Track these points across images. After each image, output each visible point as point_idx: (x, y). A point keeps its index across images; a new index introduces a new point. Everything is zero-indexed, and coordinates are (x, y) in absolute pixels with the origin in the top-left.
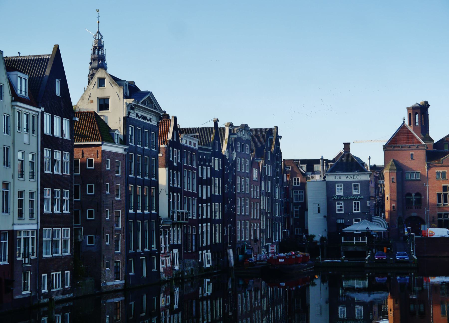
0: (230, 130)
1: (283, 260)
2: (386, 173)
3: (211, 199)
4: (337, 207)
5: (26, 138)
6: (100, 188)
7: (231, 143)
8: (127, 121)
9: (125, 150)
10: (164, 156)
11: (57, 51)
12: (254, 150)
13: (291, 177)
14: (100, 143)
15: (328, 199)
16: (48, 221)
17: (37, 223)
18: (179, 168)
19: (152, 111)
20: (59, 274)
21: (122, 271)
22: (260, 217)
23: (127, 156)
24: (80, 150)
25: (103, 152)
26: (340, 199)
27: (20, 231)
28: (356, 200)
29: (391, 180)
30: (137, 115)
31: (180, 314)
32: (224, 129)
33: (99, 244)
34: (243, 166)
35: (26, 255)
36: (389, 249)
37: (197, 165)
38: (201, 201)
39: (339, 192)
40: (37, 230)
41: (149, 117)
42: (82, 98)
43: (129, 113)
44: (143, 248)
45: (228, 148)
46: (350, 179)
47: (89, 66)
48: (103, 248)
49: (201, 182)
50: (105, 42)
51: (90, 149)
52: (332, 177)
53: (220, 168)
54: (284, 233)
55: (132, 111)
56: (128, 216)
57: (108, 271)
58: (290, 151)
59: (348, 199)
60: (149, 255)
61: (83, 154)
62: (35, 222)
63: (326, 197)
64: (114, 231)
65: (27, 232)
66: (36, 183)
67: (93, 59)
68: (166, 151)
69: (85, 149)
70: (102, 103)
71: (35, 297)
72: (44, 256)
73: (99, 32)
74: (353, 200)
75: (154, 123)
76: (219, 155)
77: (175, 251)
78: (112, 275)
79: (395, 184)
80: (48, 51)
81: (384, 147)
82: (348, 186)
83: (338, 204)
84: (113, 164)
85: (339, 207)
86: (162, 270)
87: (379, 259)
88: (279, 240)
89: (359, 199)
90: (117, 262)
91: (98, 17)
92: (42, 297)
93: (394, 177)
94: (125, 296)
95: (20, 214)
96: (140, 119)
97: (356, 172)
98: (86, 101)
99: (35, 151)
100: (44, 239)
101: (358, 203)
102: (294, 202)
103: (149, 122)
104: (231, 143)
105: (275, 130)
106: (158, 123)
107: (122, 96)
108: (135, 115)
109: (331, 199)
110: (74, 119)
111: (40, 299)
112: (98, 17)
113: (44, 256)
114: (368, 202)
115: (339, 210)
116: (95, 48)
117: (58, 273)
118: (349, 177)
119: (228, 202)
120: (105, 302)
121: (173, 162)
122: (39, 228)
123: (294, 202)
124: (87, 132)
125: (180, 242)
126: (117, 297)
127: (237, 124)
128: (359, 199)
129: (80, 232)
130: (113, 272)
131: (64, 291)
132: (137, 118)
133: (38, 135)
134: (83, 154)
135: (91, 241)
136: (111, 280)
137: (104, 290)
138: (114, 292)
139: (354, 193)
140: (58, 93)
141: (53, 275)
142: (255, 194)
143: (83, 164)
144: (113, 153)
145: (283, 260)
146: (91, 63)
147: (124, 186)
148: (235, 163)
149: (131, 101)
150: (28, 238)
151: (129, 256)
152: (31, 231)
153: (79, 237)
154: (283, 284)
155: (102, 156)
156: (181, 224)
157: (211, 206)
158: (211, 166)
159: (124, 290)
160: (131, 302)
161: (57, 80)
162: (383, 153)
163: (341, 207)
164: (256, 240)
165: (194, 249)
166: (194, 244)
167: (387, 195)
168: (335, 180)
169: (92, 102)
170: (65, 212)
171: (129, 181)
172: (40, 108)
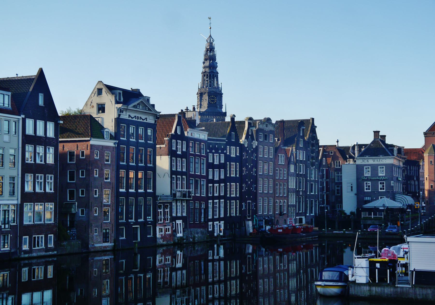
0: (249, 124)
1: (281, 231)
2: (426, 155)
3: (227, 180)
4: (380, 186)
5: (6, 138)
6: (89, 173)
7: (250, 134)
8: (118, 121)
9: (115, 144)
10: (167, 146)
11: (41, 73)
12: (280, 139)
13: (332, 160)
14: (89, 139)
15: (358, 179)
16: (27, 198)
17: (18, 199)
18: (185, 155)
19: (146, 112)
20: (42, 237)
21: (112, 236)
22: (288, 195)
23: (118, 148)
24: (62, 144)
25: (92, 146)
26: (368, 180)
28: (381, 180)
29: (430, 163)
30: (129, 116)
31: (184, 272)
32: (244, 122)
33: (88, 215)
34: (266, 152)
36: (402, 223)
37: (207, 153)
38: (209, 181)
39: (367, 174)
40: (17, 204)
41: (144, 117)
42: (86, 104)
43: (119, 115)
44: (136, 219)
45: (247, 138)
46: (376, 162)
47: (202, 65)
48: (91, 218)
49: (211, 166)
50: (216, 45)
51: (82, 143)
52: (361, 161)
53: (238, 154)
54: (322, 209)
55: (121, 113)
56: (118, 194)
57: (96, 236)
58: (325, 138)
59: (375, 180)
60: (144, 225)
61: (77, 147)
62: (16, 198)
63: (356, 178)
64: (103, 206)
66: (17, 170)
67: (206, 60)
68: (169, 143)
69: (78, 143)
70: (100, 106)
71: (15, 253)
73: (210, 36)
74: (379, 180)
75: (153, 122)
76: (237, 143)
77: (179, 222)
78: (101, 239)
79: (433, 166)
80: (34, 73)
81: (425, 134)
82: (374, 168)
83: (366, 183)
84: (102, 155)
85: (367, 187)
86: (158, 235)
87: (371, 231)
88: (315, 213)
89: (384, 180)
90: (106, 229)
91: (210, 24)
92: (23, 253)
93: (433, 160)
94: (114, 255)
96: (134, 119)
97: (381, 157)
98: (89, 106)
99: (16, 147)
101: (383, 183)
102: (336, 181)
103: (145, 121)
104: (250, 134)
105: (311, 121)
106: (155, 121)
107: (114, 102)
108: (128, 116)
109: (360, 180)
110: (58, 122)
112: (210, 24)
114: (392, 182)
115: (381, 189)
116: (207, 50)
117: (40, 236)
118: (376, 160)
119: (247, 182)
120: (93, 259)
121: (177, 150)
122: (19, 202)
123: (336, 181)
124: (81, 130)
125: (185, 214)
126: (105, 255)
127: (258, 116)
128: (384, 180)
129: (74, 206)
130: (102, 237)
131: (47, 249)
132: (130, 119)
133: (19, 135)
134: (77, 147)
135: (82, 213)
136: (100, 243)
137: (92, 250)
138: (104, 251)
139: (380, 175)
140: (41, 102)
141: (35, 238)
142: (281, 175)
143: (78, 156)
144: (102, 146)
145: (281, 231)
146: (204, 63)
147: (114, 171)
148: (256, 150)
149: (120, 106)
151: (118, 225)
153: (73, 209)
154: (281, 250)
155: (91, 149)
156: (187, 200)
157: (226, 187)
158: (225, 154)
159: (114, 251)
160: (122, 259)
162: (424, 138)
163: (383, 186)
164: (281, 214)
165: (202, 220)
166: (203, 216)
167: (426, 175)
168: (364, 163)
169: (93, 107)
171: (119, 167)
172: (20, 116)
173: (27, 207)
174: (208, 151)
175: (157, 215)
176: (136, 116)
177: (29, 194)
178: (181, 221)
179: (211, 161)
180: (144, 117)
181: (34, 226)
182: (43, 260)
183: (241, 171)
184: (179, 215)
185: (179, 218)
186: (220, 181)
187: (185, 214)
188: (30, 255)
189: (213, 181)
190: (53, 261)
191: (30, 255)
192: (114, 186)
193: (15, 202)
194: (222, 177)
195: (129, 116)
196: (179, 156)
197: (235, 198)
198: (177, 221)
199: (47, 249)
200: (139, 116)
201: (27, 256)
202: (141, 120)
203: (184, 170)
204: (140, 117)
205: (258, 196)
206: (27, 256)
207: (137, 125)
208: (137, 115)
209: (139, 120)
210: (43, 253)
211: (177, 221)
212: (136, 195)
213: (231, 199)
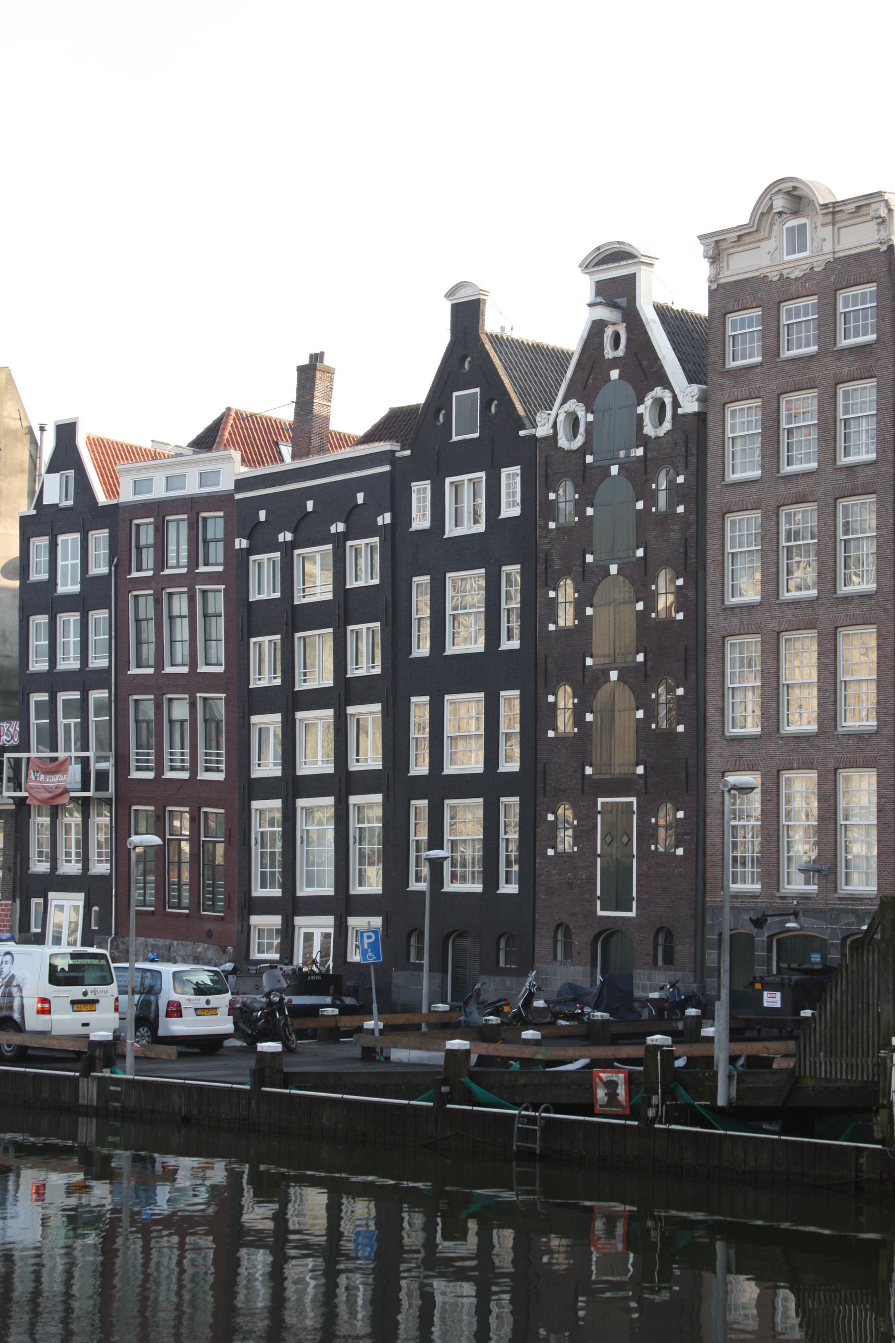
18: (92, 595)
174: (241, 543)
178: (82, 896)
179: (263, 588)
183: (535, 610)
184: (71, 867)
185: (67, 884)
186: (344, 693)
187: (101, 868)
189: (289, 701)
194: (366, 664)
197: (487, 785)
198: (51, 895)
203: (99, 661)
205: (714, 760)
211: (51, 895)
213: (442, 787)
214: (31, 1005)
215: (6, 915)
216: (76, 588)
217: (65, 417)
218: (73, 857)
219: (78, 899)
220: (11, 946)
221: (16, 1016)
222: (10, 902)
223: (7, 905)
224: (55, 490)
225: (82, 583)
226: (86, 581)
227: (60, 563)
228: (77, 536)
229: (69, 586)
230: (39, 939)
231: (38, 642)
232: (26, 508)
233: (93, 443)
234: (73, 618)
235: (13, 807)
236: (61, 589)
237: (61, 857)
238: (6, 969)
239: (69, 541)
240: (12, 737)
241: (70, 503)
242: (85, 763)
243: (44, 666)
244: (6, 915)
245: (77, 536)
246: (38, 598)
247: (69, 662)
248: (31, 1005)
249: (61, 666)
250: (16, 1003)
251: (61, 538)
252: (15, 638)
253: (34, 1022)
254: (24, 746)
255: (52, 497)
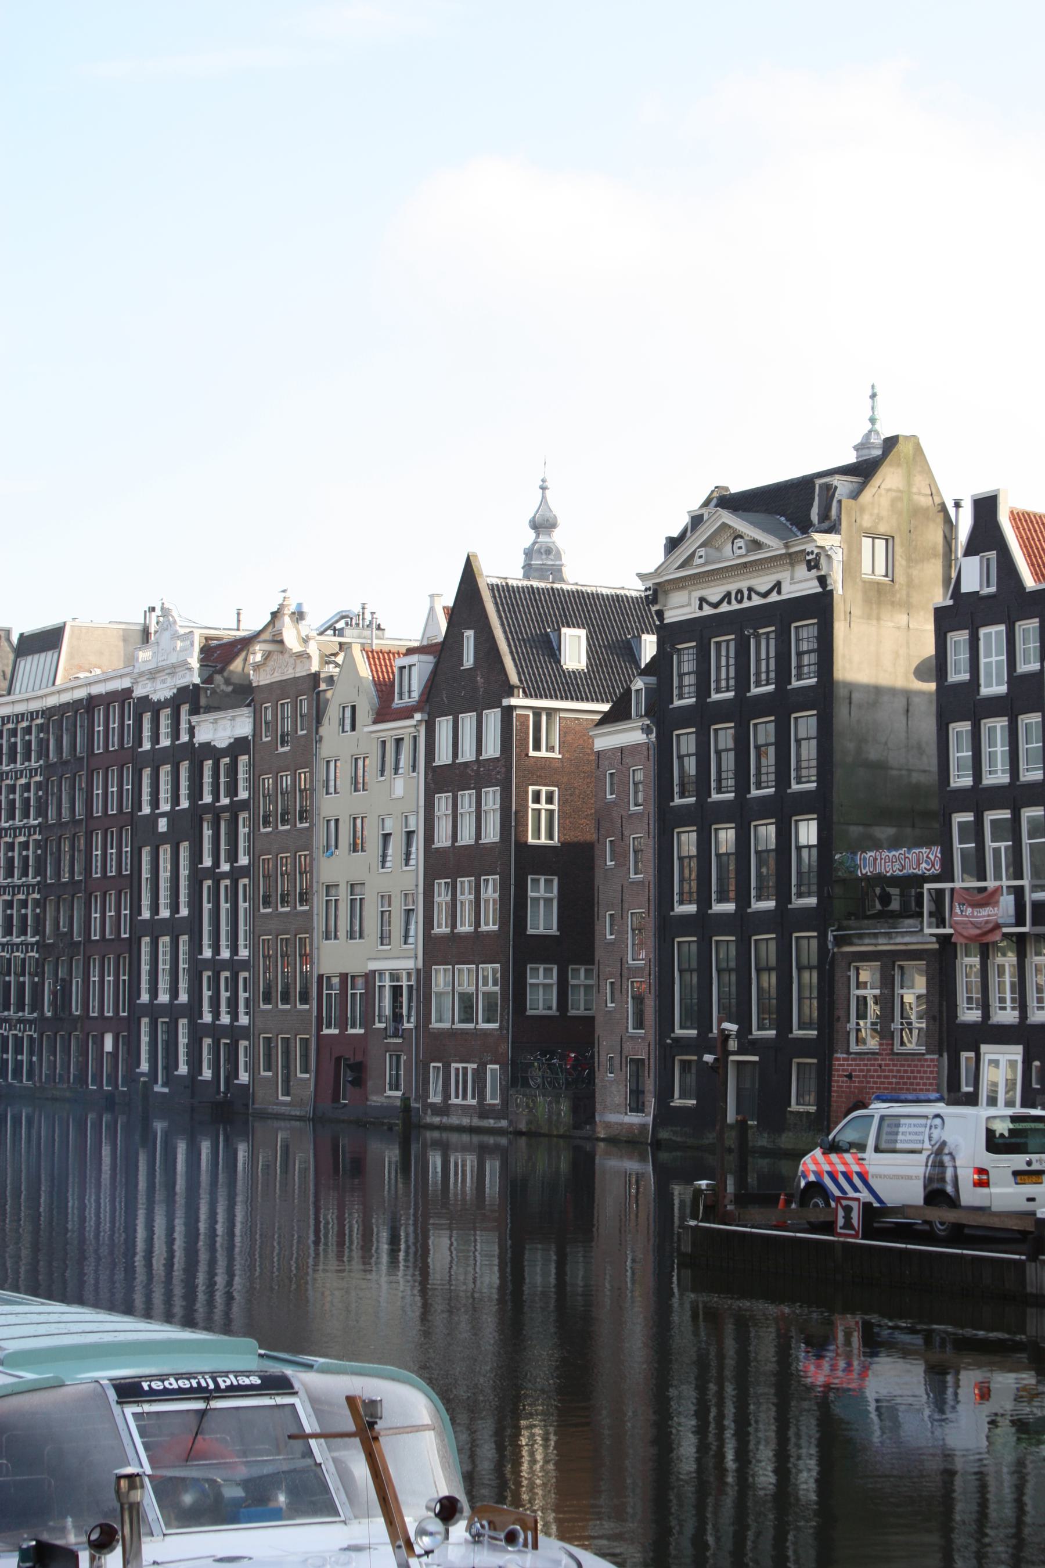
9: (647, 730)
18: (1023, 696)
19: (745, 565)
27: (381, 973)
35: (397, 1017)
56: (667, 929)
64: (625, 972)
65: (395, 976)
72: (435, 1025)
92: (429, 1111)
95: (384, 938)
96: (724, 608)
100: (434, 989)
103: (774, 597)
111: (426, 1114)
113: (435, 1025)
122: (420, 965)
132: (708, 611)
141: (457, 1069)
144: (622, 749)
147: (651, 839)
150: (401, 986)
152: (387, 973)
161: (469, 634)
170: (484, 928)
172: (412, 717)
173: (440, 978)
175: (840, 1013)
176: (728, 595)
177: (443, 937)
178: (1020, 1048)
180: (763, 583)
181: (452, 1033)
182: (476, 1139)
184: (1006, 1016)
185: (1003, 1035)
188: (445, 1120)
190: (497, 1147)
191: (445, 1120)
192: (652, 898)
193: (410, 964)
195: (702, 600)
196: (995, 706)
198: (984, 1048)
199: (484, 1112)
200: (744, 585)
201: (436, 1120)
202: (757, 601)
204: (750, 590)
206: (436, 1120)
207: (741, 623)
208: (733, 587)
209: (746, 604)
210: (476, 1122)
211: (984, 1048)
212: (743, 924)
214: (967, 1177)
215: (932, 1072)
216: (1003, 689)
217: (983, 489)
218: (1008, 1004)
219: (1015, 1053)
220: (940, 1108)
221: (949, 1189)
222: (936, 1057)
223: (932, 1060)
224: (973, 576)
225: (1009, 683)
226: (1015, 680)
227: (983, 660)
228: (1002, 628)
229: (993, 687)
230: (972, 1100)
231: (960, 754)
232: (940, 598)
233: (1020, 518)
234: (1000, 724)
235: (936, 946)
236: (985, 691)
237: (994, 1003)
238: (936, 1134)
239: (993, 634)
240: (933, 865)
241: (993, 589)
242: (1018, 893)
243: (967, 782)
244: (932, 1072)
245: (1002, 628)
246: (958, 702)
247: (997, 776)
248: (967, 1177)
249: (988, 780)
250: (949, 1174)
251: (983, 631)
252: (932, 749)
253: (970, 1196)
254: (946, 874)
255: (971, 583)
